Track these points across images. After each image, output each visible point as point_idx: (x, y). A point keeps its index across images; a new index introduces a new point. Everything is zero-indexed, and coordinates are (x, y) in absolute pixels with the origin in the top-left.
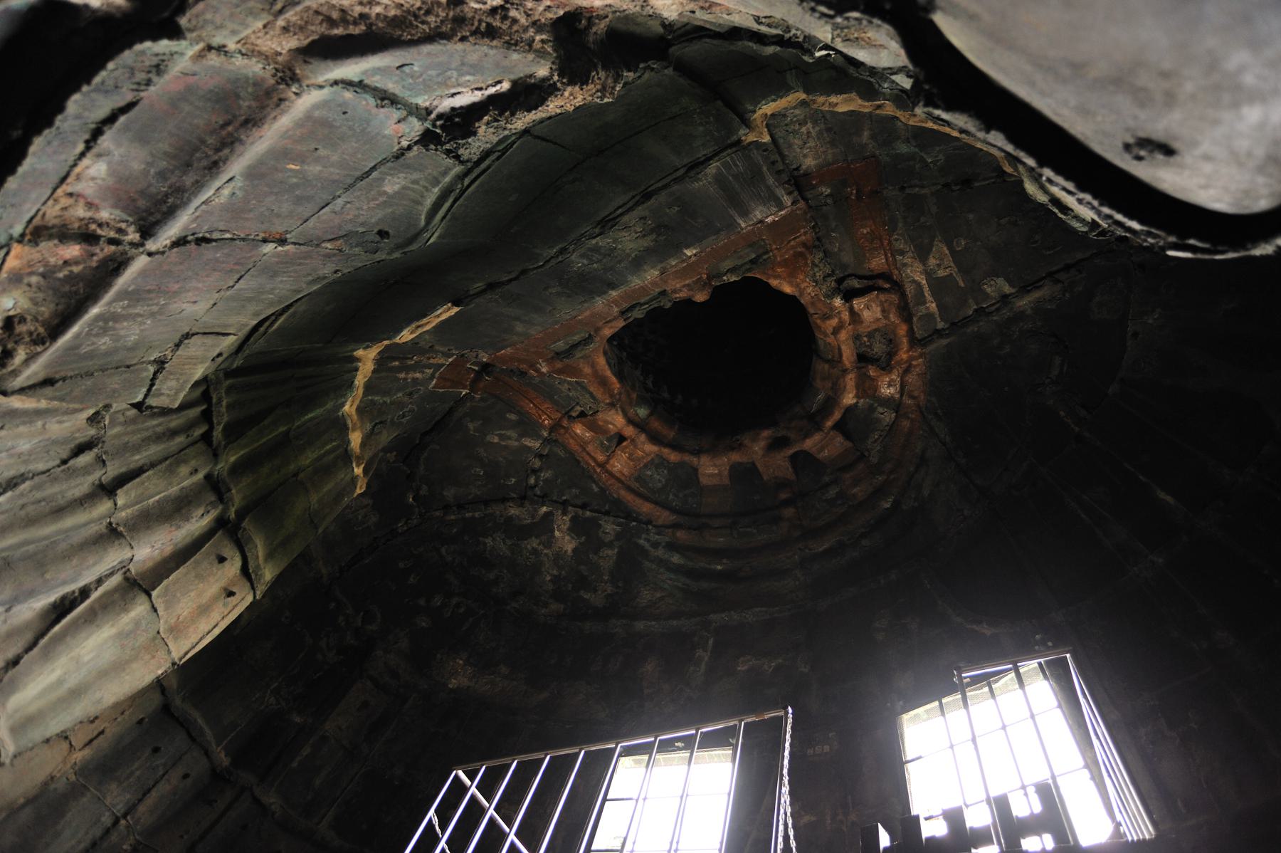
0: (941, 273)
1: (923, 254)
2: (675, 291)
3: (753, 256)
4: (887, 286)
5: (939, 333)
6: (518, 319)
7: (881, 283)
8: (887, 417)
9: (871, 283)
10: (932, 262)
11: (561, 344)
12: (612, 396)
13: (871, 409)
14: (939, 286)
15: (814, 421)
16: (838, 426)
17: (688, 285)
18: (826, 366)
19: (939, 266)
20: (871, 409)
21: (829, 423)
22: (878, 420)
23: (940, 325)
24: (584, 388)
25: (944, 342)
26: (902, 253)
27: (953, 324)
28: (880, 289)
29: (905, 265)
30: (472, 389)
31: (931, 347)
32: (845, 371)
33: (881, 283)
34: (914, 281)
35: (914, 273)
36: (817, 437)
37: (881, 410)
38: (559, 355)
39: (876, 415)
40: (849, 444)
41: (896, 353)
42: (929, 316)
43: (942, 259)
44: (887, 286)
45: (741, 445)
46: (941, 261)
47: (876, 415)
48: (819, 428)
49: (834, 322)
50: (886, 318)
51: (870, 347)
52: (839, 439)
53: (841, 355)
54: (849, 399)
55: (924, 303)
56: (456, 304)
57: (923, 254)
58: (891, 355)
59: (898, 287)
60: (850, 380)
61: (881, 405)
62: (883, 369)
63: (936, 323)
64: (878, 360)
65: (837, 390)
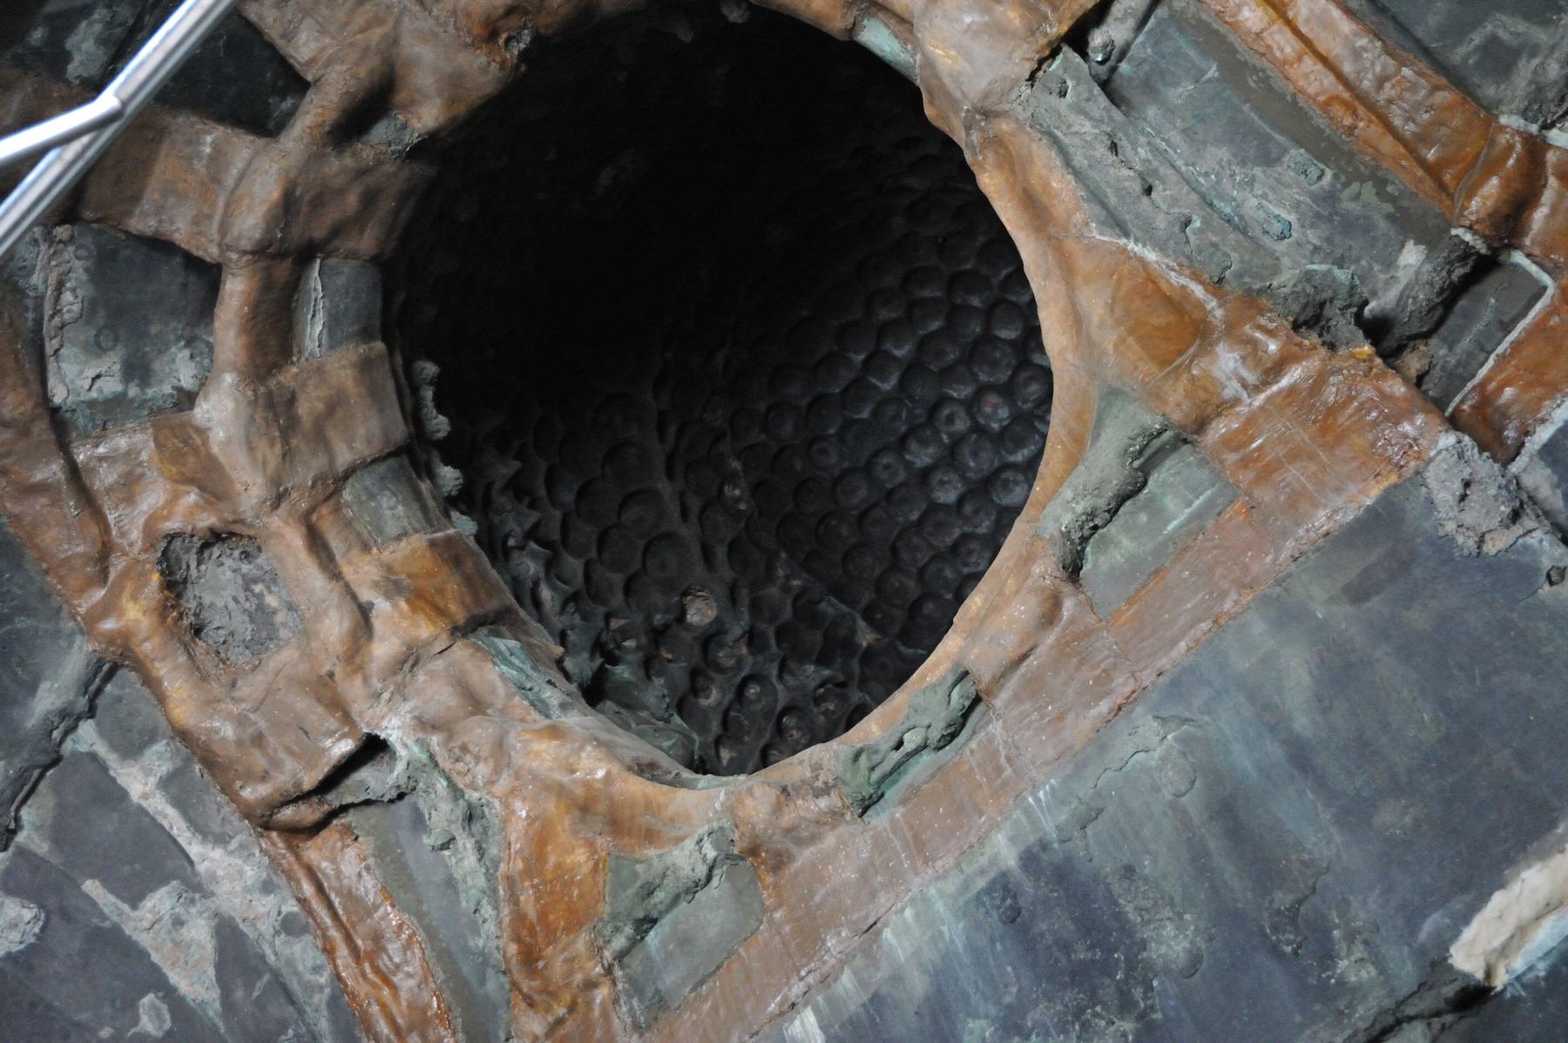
0: (161, 901)
1: (233, 946)
2: (836, 816)
3: (653, 938)
4: (287, 814)
5: (69, 719)
6: (1301, 757)
7: (307, 813)
8: (78, 376)
9: (334, 799)
10: (200, 932)
11: (1178, 515)
12: (997, 143)
13: (137, 370)
14: (149, 861)
15: (288, 256)
16: (209, 276)
17: (800, 842)
18: (344, 457)
19: (178, 923)
20: (137, 370)
21: (236, 290)
22: (97, 349)
23: (87, 737)
24: (1097, 197)
25: (47, 700)
26: (289, 926)
27: (56, 761)
28: (304, 797)
29: (267, 887)
30: (1535, 148)
31: (73, 662)
32: (278, 500)
33: (307, 813)
34: (221, 840)
35: (233, 871)
36: (250, 223)
37: (111, 386)
38: (1186, 435)
39: (112, 363)
40: (142, 223)
41: (163, 611)
42: (131, 749)
43: (177, 944)
44: (287, 814)
45: (492, 35)
46: (172, 935)
47: (112, 363)
48: (263, 252)
49: (383, 648)
50: (241, 721)
51: (248, 583)
52: (180, 231)
53: (316, 542)
54: (221, 412)
55: (165, 783)
56: (1474, 997)
57: (233, 946)
58: (174, 585)
59: (263, 820)
60: (250, 487)
61: (118, 400)
62: (172, 537)
63: (102, 733)
64: (206, 546)
65: (276, 412)
